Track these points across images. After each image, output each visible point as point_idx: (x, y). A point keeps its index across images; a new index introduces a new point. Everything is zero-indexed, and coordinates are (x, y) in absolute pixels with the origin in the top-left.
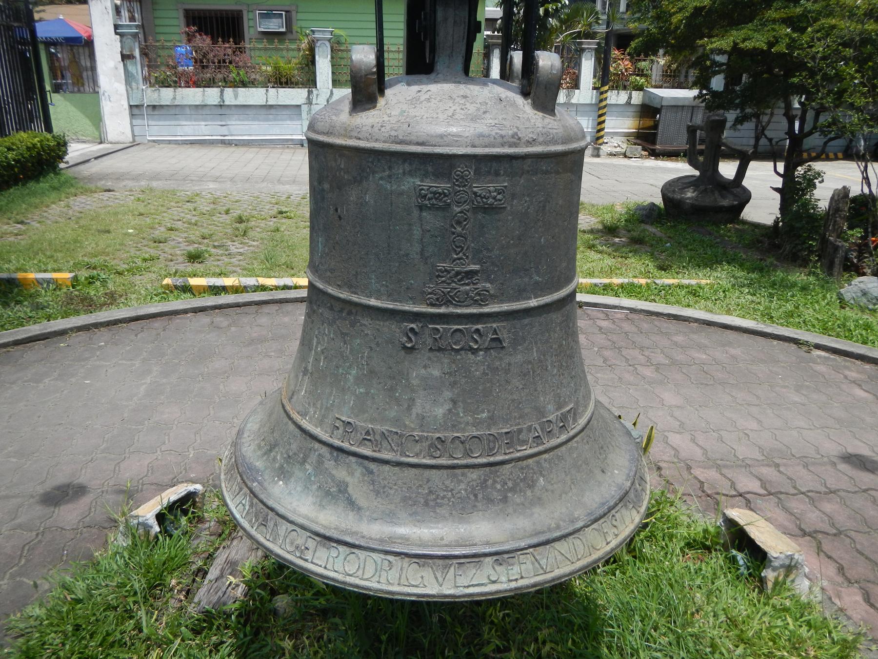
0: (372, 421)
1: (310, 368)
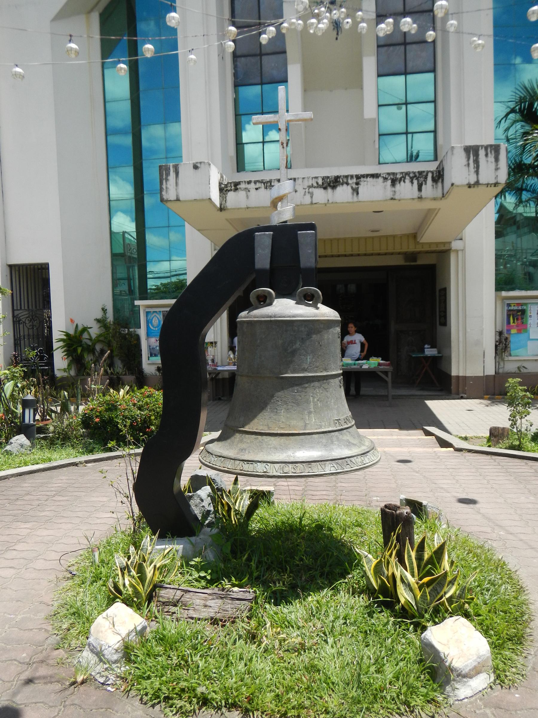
0: (343, 415)
1: (312, 410)
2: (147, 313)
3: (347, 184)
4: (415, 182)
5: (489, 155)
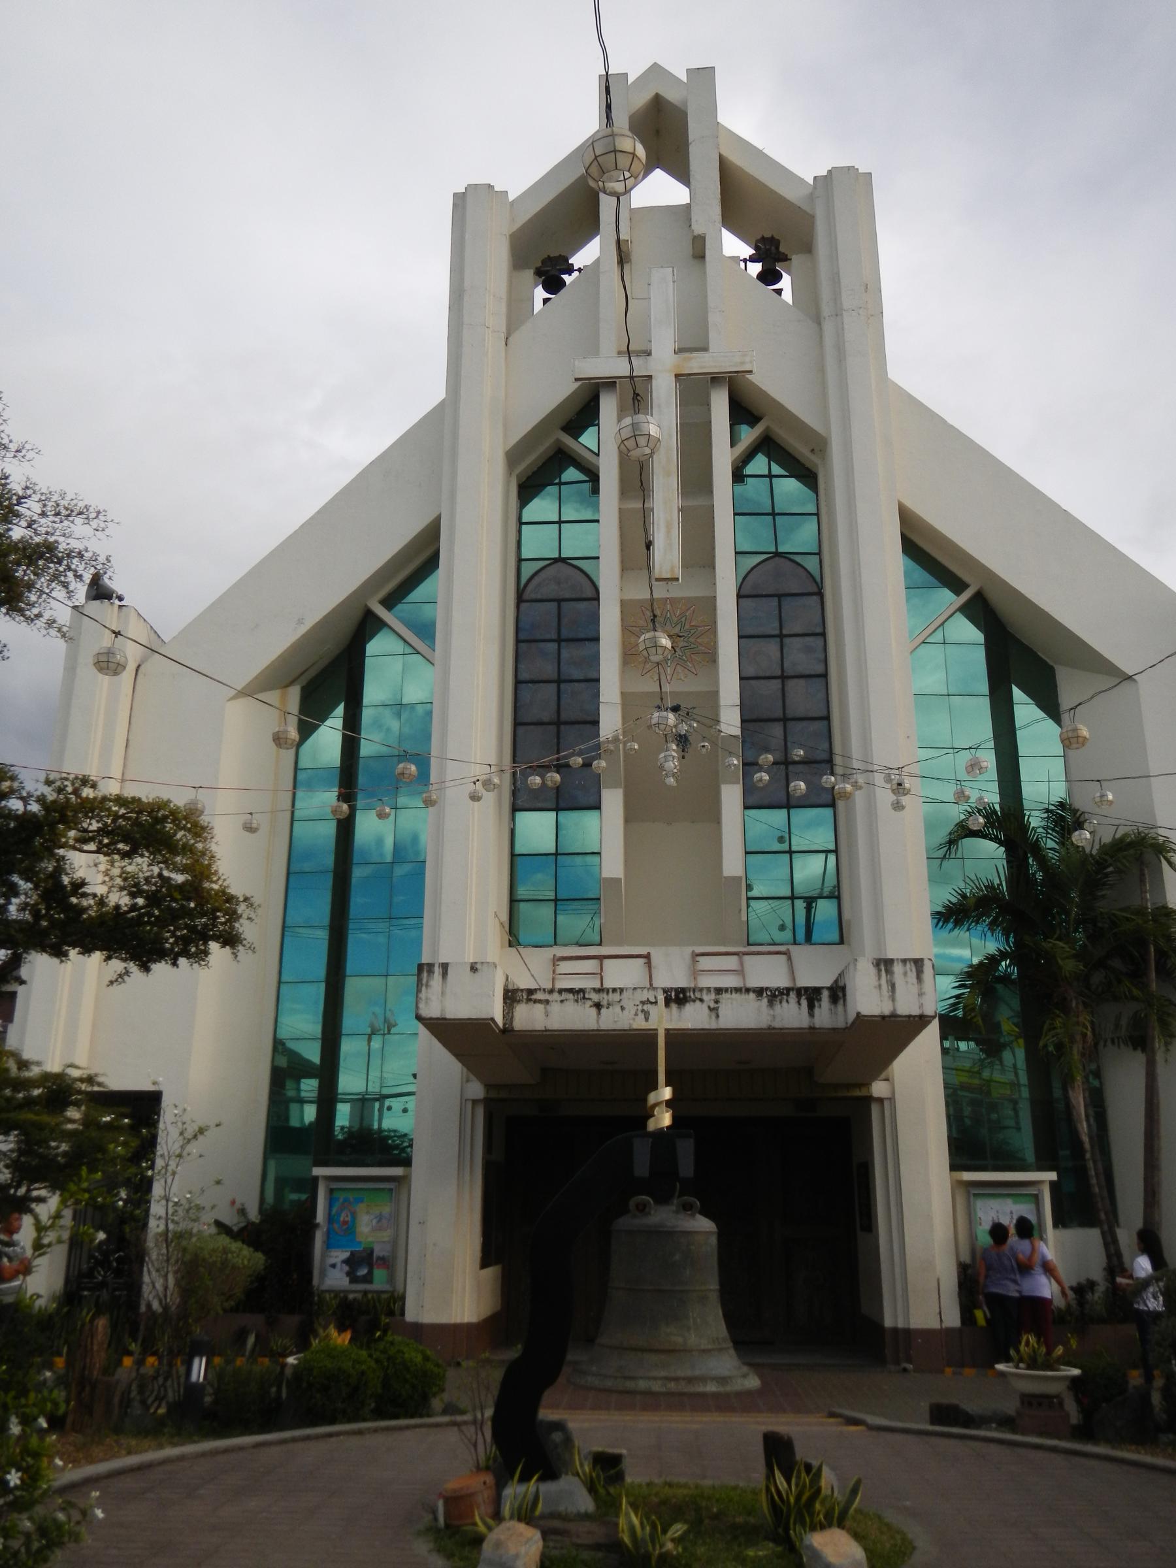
2: (332, 1191)
3: (701, 1000)
4: (804, 1002)
5: (909, 973)
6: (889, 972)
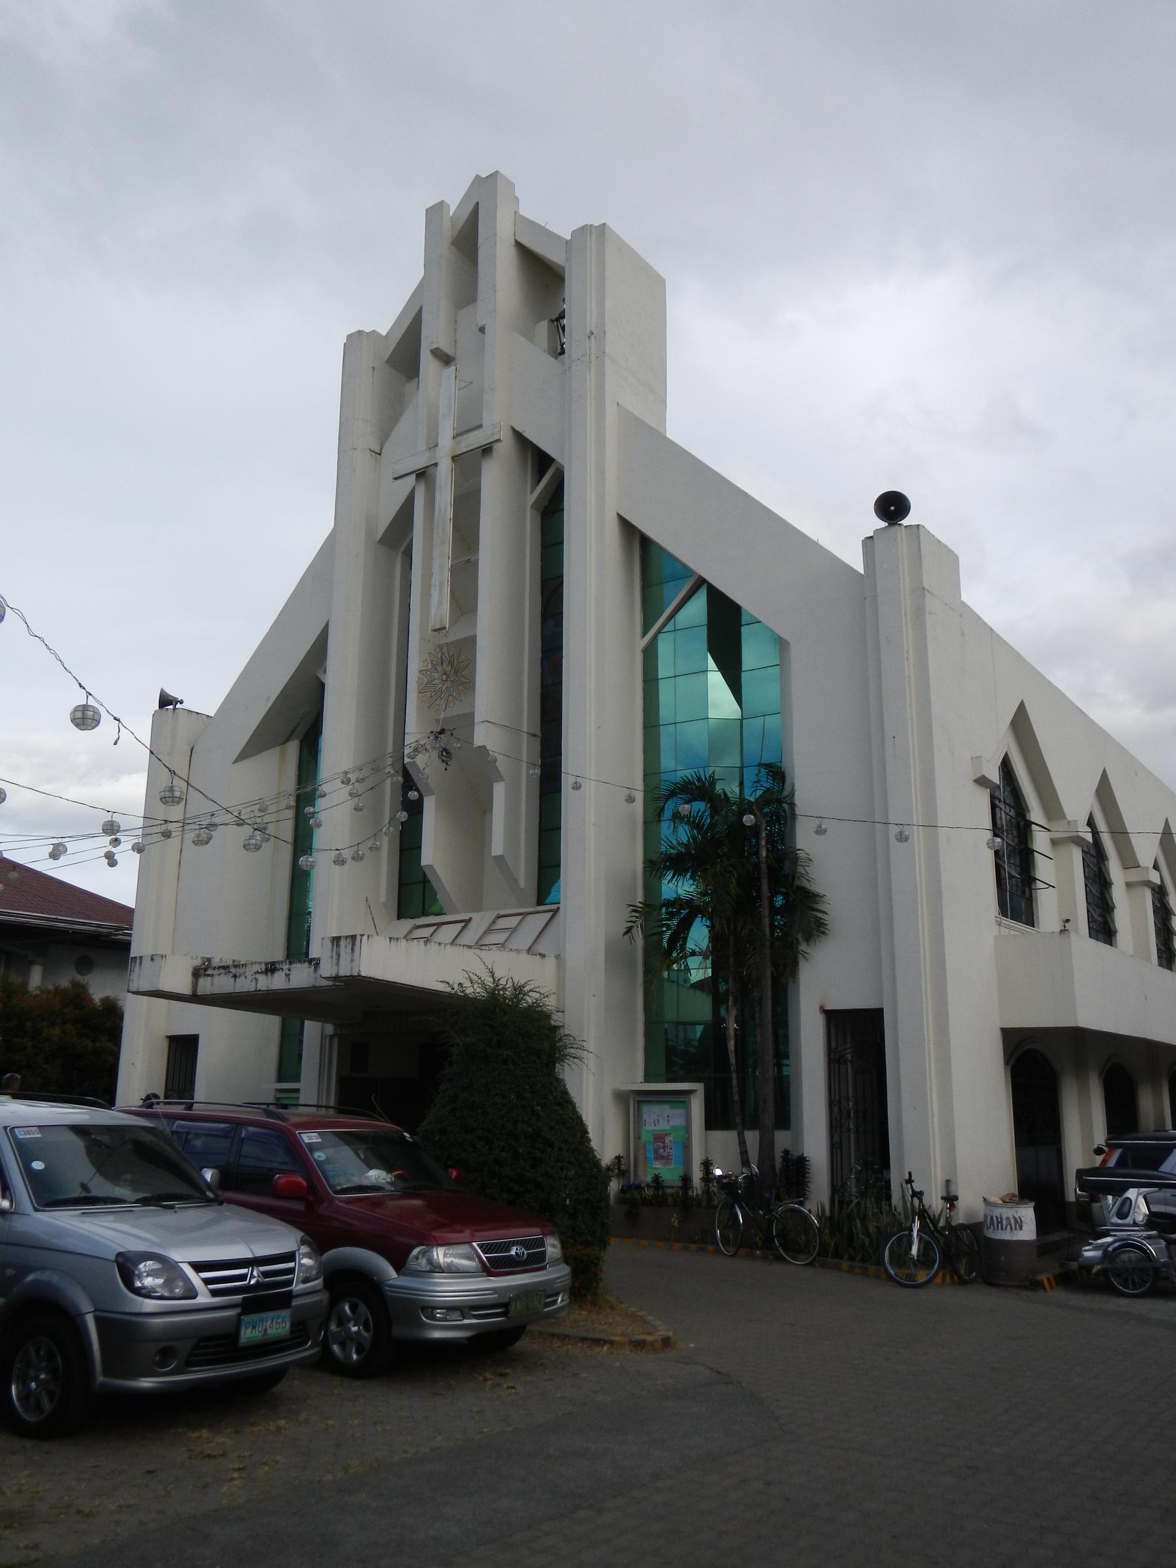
6: (338, 946)
